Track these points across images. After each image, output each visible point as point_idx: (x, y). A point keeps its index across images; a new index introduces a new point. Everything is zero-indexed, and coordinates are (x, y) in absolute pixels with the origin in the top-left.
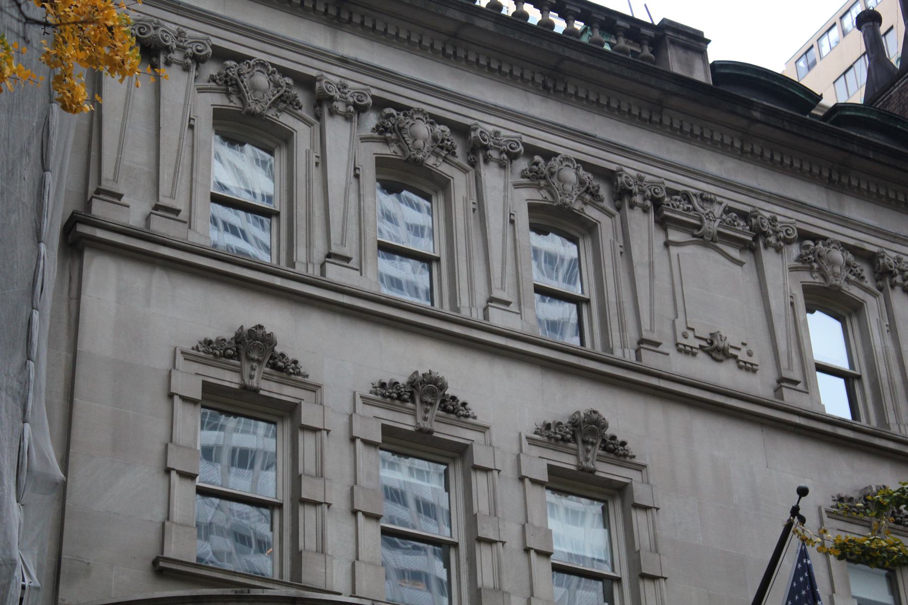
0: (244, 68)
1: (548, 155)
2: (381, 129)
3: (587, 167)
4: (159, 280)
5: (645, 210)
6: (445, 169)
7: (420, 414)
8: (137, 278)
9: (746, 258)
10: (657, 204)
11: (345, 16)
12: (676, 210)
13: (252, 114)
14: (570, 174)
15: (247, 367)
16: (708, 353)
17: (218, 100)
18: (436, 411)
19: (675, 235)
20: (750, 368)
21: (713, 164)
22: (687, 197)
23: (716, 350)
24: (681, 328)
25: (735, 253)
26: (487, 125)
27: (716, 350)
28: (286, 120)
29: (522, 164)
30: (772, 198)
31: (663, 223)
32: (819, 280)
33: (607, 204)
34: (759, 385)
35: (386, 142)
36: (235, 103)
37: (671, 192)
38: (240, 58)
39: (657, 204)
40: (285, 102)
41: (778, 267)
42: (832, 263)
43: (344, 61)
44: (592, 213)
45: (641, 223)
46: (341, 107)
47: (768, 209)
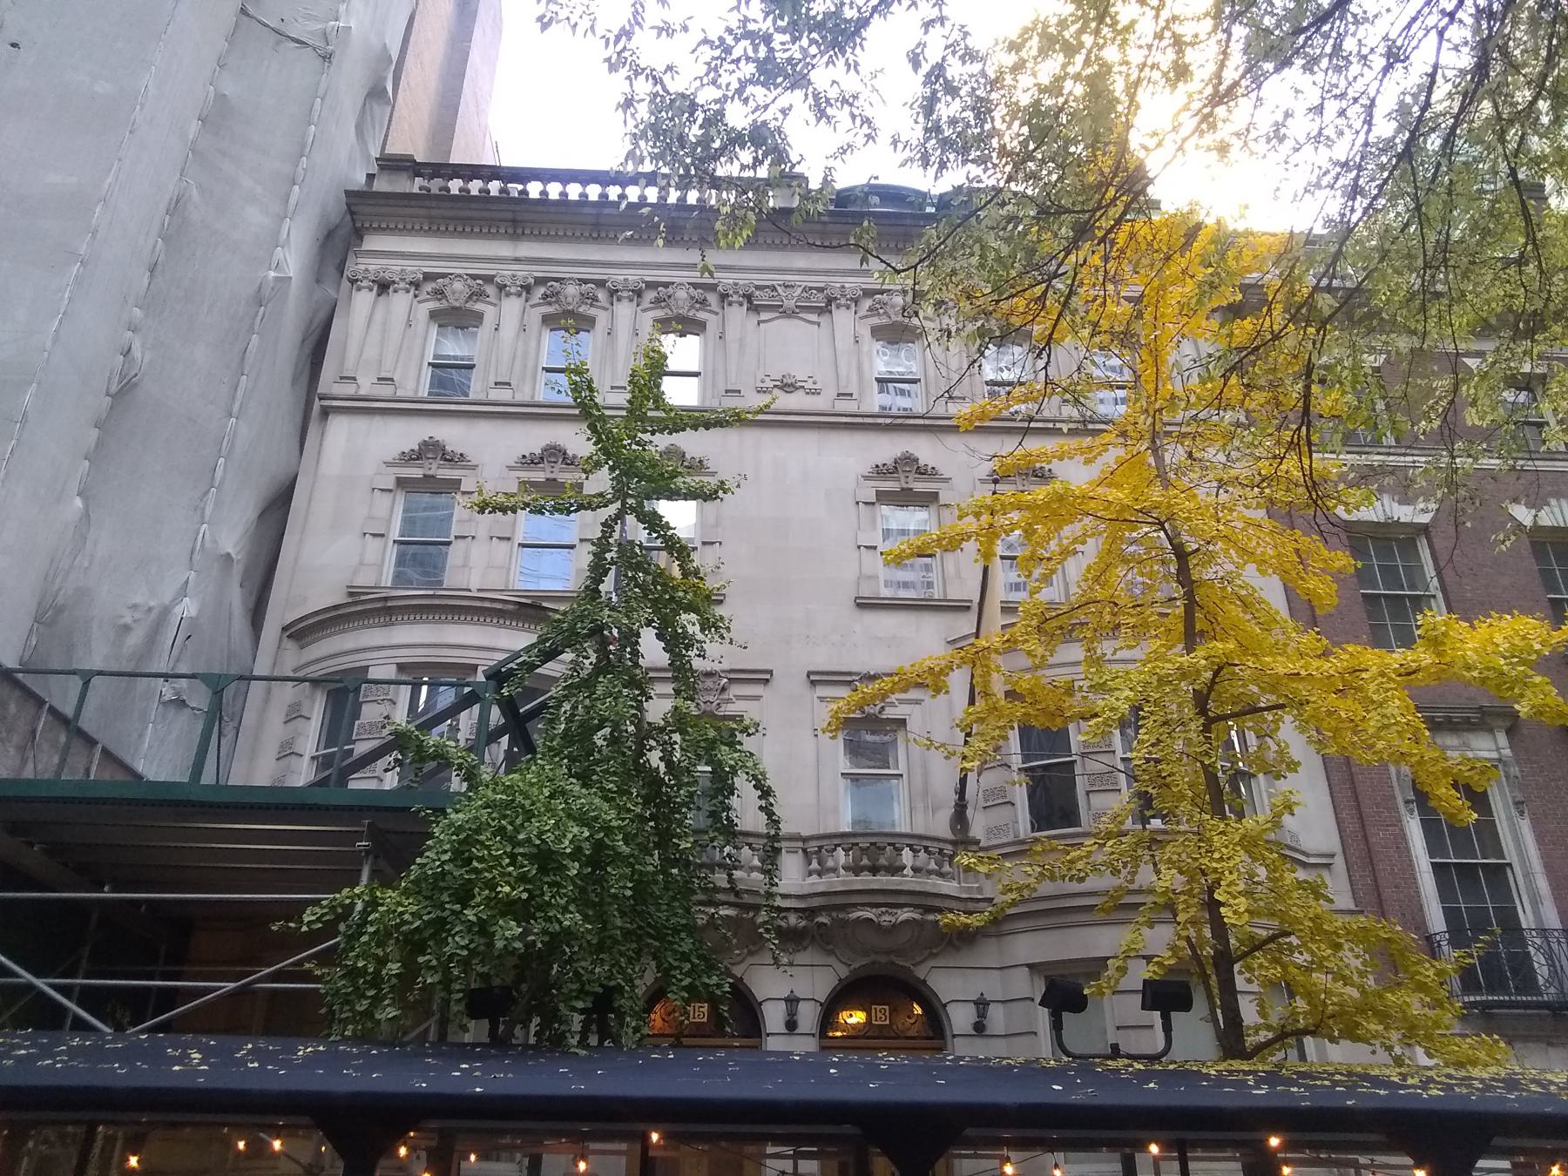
0: (447, 281)
1: (666, 285)
2: (545, 296)
3: (695, 286)
4: (378, 422)
5: (741, 304)
6: (592, 312)
7: (903, 480)
8: (360, 424)
9: (824, 320)
10: (749, 297)
11: (519, 231)
12: (762, 298)
13: (454, 308)
14: (682, 294)
15: (426, 463)
16: (780, 388)
17: (433, 305)
18: (559, 465)
19: (764, 316)
20: (816, 392)
21: (800, 260)
22: (774, 289)
23: (788, 387)
24: (760, 376)
25: (813, 317)
26: (617, 276)
27: (788, 387)
28: (479, 307)
29: (650, 295)
30: (827, 272)
31: (755, 309)
32: (885, 320)
33: (715, 307)
34: (819, 403)
35: (550, 304)
36: (444, 304)
37: (758, 288)
38: (444, 276)
39: (749, 297)
40: (479, 295)
41: (843, 319)
42: (893, 307)
43: (517, 260)
44: (702, 315)
45: (737, 315)
46: (513, 290)
47: (837, 282)
